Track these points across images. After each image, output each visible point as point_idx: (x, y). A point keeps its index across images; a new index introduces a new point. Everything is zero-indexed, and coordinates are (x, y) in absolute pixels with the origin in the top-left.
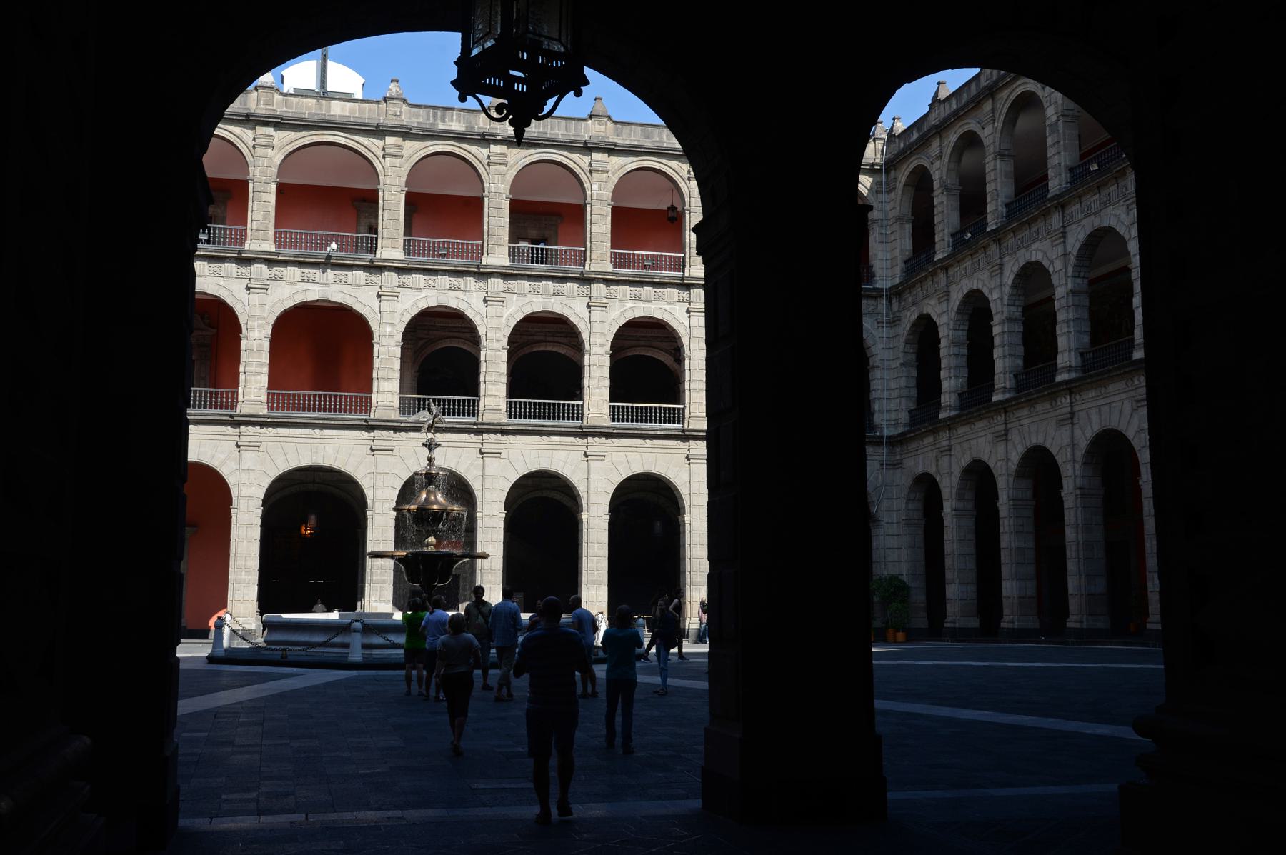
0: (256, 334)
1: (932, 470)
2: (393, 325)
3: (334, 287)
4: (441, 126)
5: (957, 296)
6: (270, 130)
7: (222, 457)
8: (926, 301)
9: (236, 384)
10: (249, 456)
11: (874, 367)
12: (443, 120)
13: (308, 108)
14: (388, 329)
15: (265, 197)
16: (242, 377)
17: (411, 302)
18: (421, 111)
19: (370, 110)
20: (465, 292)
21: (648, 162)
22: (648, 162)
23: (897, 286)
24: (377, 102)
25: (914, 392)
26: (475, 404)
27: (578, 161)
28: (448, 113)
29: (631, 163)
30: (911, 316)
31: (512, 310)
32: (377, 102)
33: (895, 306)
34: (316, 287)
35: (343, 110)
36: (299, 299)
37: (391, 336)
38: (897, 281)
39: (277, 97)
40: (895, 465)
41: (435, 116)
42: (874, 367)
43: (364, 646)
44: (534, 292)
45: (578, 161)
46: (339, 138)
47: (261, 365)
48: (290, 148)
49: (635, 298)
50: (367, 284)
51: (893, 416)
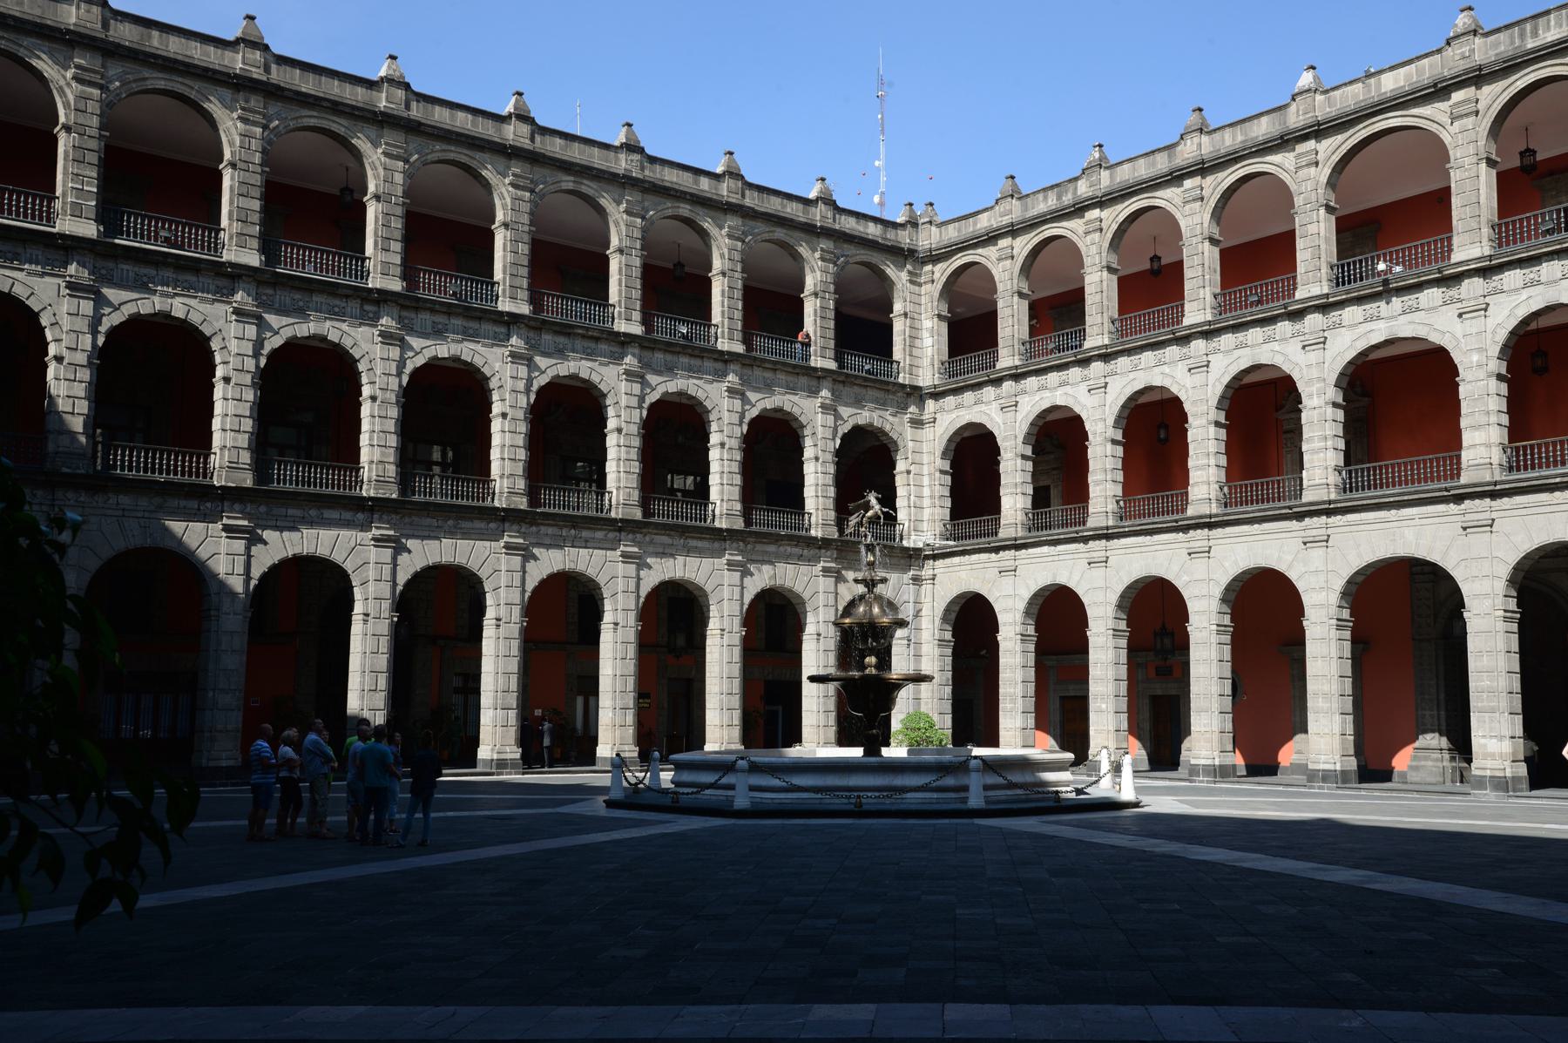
0: (1315, 402)
2: (1480, 350)
4: (1531, 44)
6: (1311, 144)
7: (1290, 558)
9: (1301, 466)
12: (1535, 34)
13: (1355, 95)
14: (1475, 358)
15: (1312, 229)
17: (1506, 312)
18: (1501, 36)
19: (1431, 66)
24: (1439, 51)
28: (1541, 21)
32: (1439, 51)
39: (1319, 98)
43: (965, 789)
50: (1445, 303)
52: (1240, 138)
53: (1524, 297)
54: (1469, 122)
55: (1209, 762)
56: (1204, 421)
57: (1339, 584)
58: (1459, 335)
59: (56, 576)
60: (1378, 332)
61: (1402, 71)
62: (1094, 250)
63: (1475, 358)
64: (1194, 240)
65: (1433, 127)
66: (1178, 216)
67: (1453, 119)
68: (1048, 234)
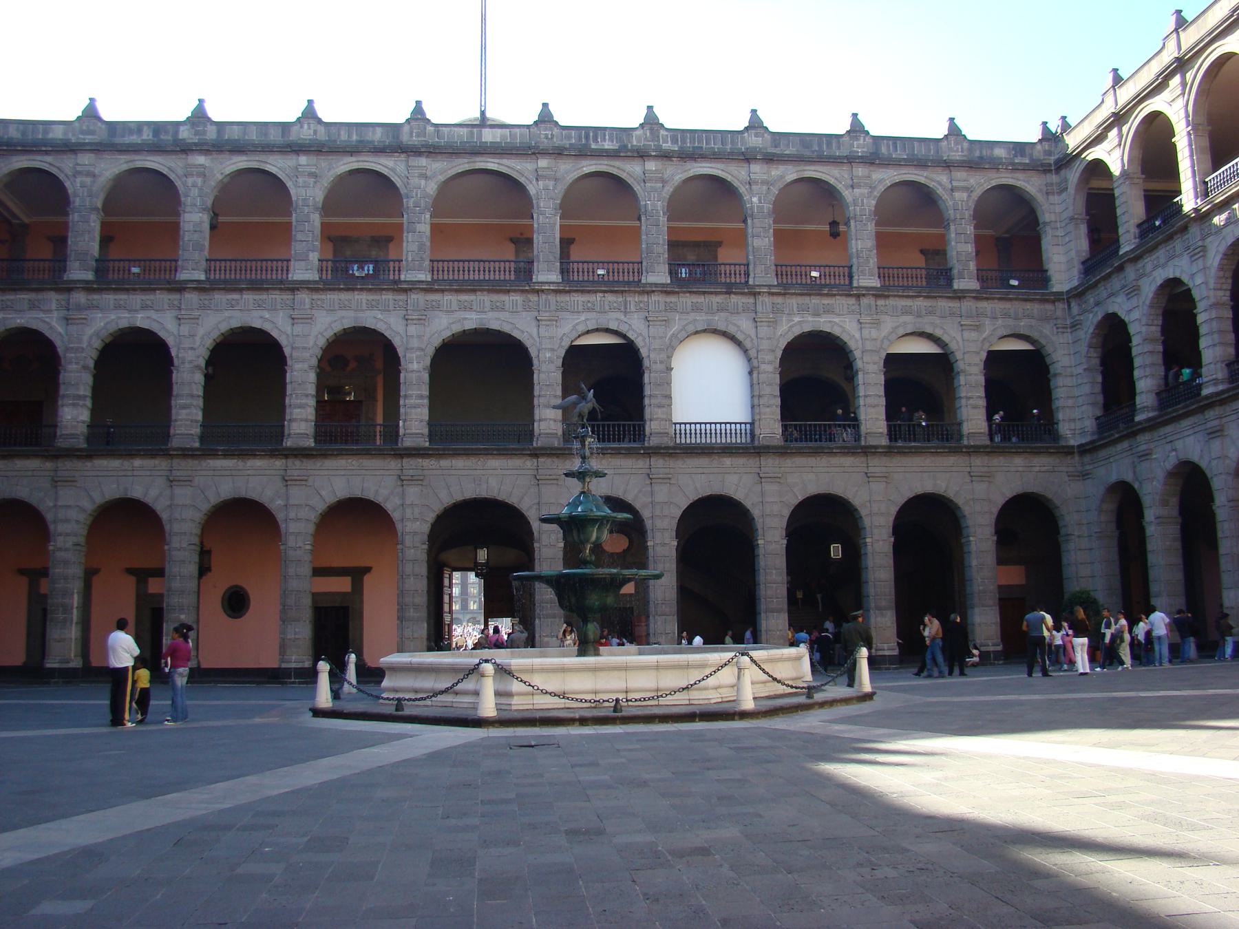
0: (415, 366)
1: (1129, 477)
2: (552, 350)
3: (491, 315)
5: (1149, 288)
6: (423, 161)
8: (1113, 299)
10: (413, 492)
11: (1055, 375)
12: (596, 140)
14: (548, 355)
16: (402, 410)
21: (812, 172)
23: (1076, 288)
25: (1100, 399)
26: (641, 429)
30: (1092, 320)
31: (675, 329)
32: (528, 127)
33: (1075, 309)
34: (473, 316)
35: (494, 136)
36: (457, 328)
37: (551, 361)
38: (1075, 283)
40: (1084, 475)
42: (1055, 375)
43: (498, 694)
44: (696, 308)
46: (492, 164)
47: (421, 397)
48: (442, 178)
49: (803, 309)
51: (1078, 425)
52: (355, 137)
53: (583, 318)
55: (300, 665)
56: (306, 366)
57: (431, 517)
58: (535, 335)
59: (1133, 416)
60: (471, 321)
62: (195, 192)
64: (306, 210)
65: (522, 180)
66: (289, 184)
68: (139, 164)
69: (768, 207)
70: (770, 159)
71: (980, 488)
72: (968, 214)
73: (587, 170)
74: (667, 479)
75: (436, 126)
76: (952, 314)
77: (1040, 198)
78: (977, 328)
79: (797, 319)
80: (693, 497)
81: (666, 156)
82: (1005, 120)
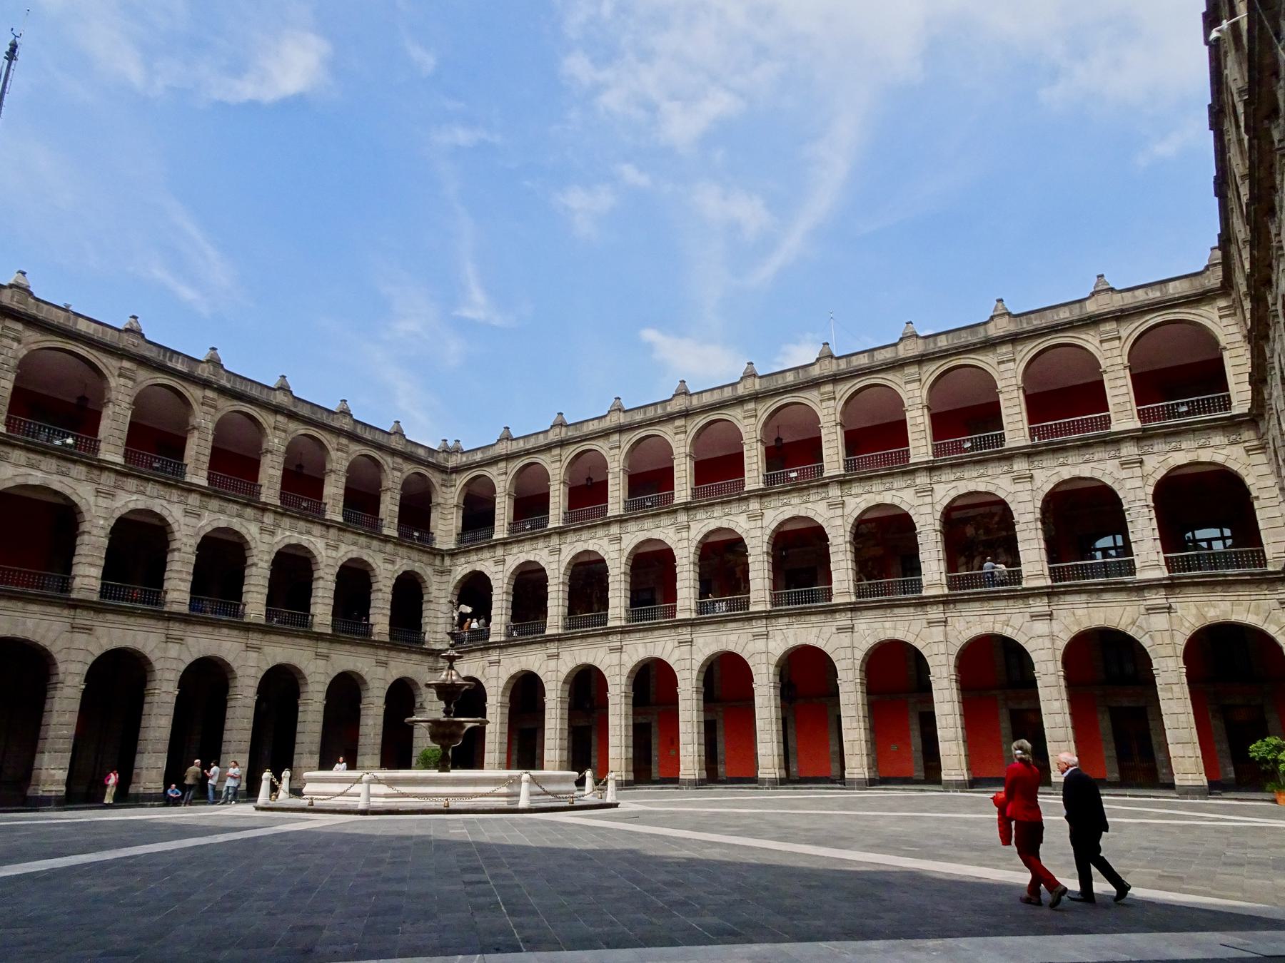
2: (105, 519)
3: (55, 477)
6: (19, 327)
14: (102, 522)
17: (123, 502)
18: (154, 349)
20: (169, 501)
21: (313, 432)
22: (313, 432)
27: (267, 419)
29: (302, 429)
31: (204, 522)
32: (119, 331)
34: (39, 474)
41: (164, 356)
44: (222, 512)
45: (267, 419)
48: (34, 347)
49: (292, 528)
54: (130, 384)
61: (94, 325)
63: (102, 522)
65: (105, 371)
67: (120, 376)
69: (283, 449)
70: (292, 416)
71: (380, 671)
72: (399, 487)
73: (160, 381)
74: (180, 640)
75: (38, 300)
76: (380, 551)
77: (437, 486)
78: (393, 562)
79: (288, 533)
80: (197, 656)
81: (222, 391)
82: (426, 433)
